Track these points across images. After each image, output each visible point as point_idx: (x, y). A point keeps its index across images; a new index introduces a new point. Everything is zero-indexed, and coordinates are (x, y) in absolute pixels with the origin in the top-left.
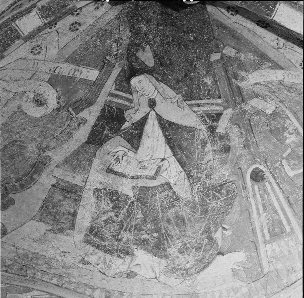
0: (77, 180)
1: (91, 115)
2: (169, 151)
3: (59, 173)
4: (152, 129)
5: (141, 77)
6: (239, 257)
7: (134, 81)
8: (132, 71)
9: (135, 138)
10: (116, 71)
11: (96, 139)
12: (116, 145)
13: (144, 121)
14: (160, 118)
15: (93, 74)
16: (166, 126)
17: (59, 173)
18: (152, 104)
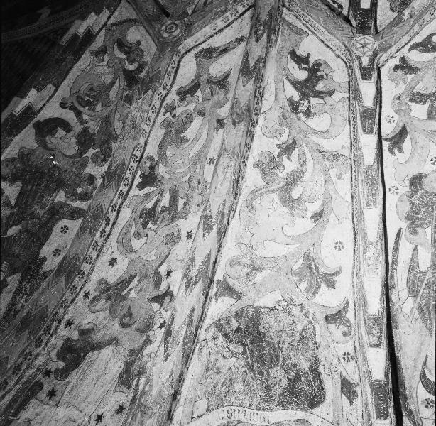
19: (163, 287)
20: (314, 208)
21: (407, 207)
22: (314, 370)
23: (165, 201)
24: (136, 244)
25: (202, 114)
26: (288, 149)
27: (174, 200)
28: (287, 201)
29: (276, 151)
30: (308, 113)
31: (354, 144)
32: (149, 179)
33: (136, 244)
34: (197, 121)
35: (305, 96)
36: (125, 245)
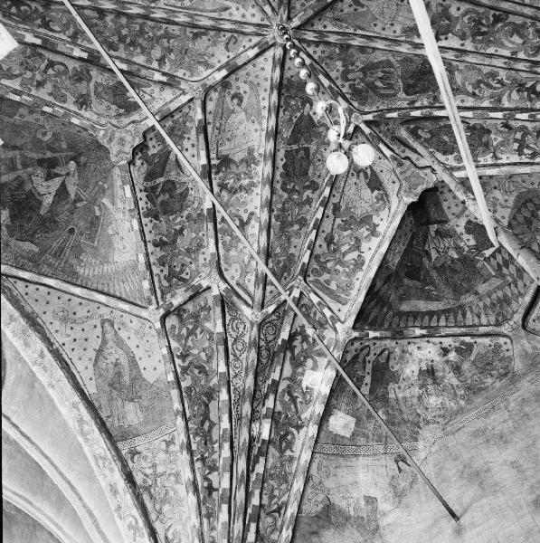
0: (19, 166)
1: (49, 155)
2: (54, 194)
3: (18, 157)
4: (58, 181)
5: (75, 164)
6: (36, 249)
7: (72, 162)
8: (73, 159)
9: (49, 177)
10: (70, 154)
11: (40, 162)
12: (40, 171)
13: (57, 175)
14: (64, 181)
15: (64, 146)
16: (63, 185)
17: (18, 157)
18: (68, 174)
19: (442, 37)
20: (477, 91)
21: (478, 127)
22: (416, 93)
23: (484, 29)
24: (466, 19)
25: (524, 43)
26: (500, 82)
27: (483, 34)
28: (479, 82)
29: (499, 78)
30: (518, 91)
31: (502, 110)
32: (497, 19)
33: (466, 19)
34: (520, 41)
35: (527, 89)
36: (466, 13)
